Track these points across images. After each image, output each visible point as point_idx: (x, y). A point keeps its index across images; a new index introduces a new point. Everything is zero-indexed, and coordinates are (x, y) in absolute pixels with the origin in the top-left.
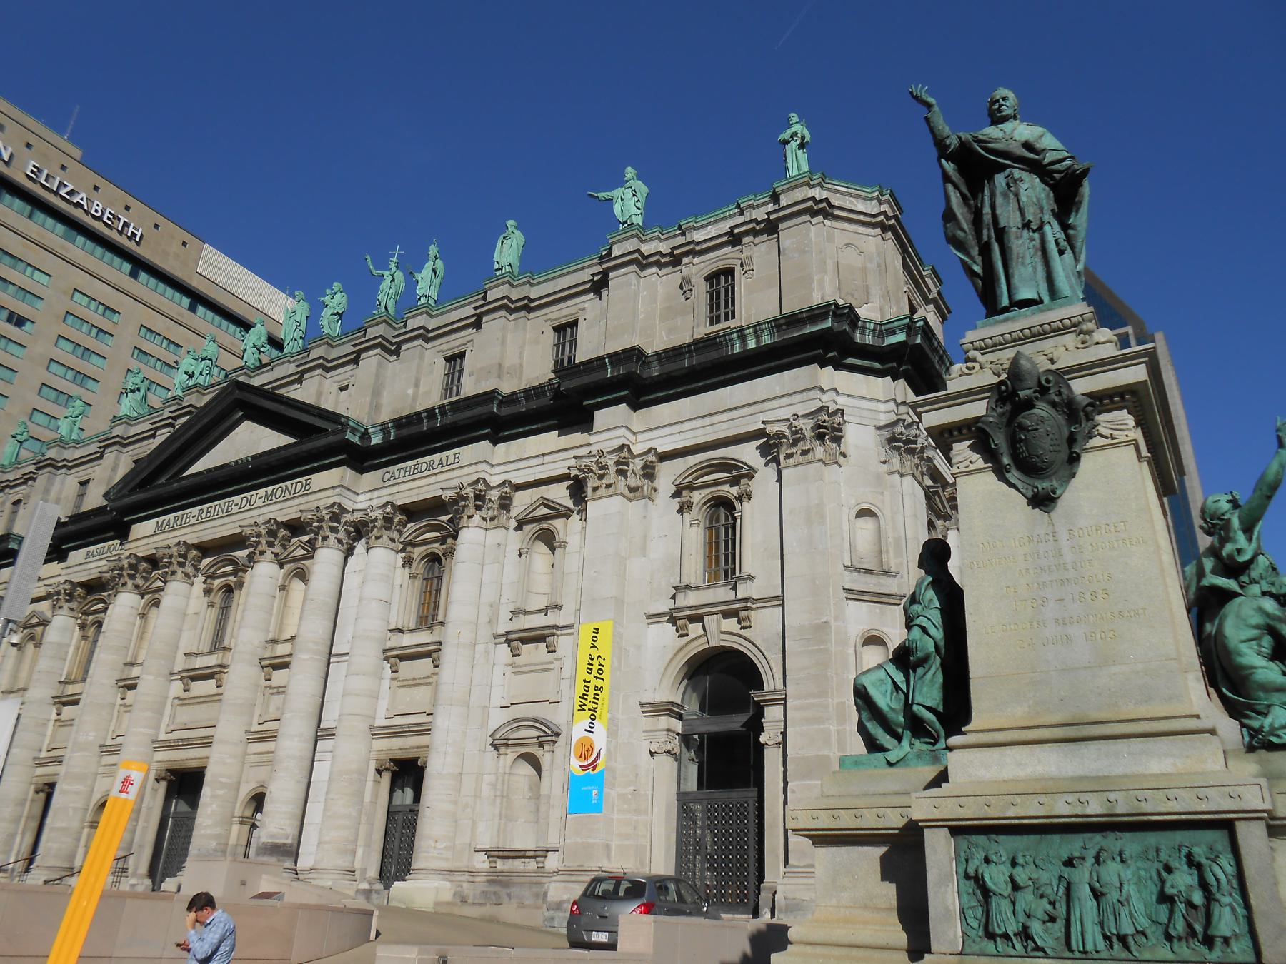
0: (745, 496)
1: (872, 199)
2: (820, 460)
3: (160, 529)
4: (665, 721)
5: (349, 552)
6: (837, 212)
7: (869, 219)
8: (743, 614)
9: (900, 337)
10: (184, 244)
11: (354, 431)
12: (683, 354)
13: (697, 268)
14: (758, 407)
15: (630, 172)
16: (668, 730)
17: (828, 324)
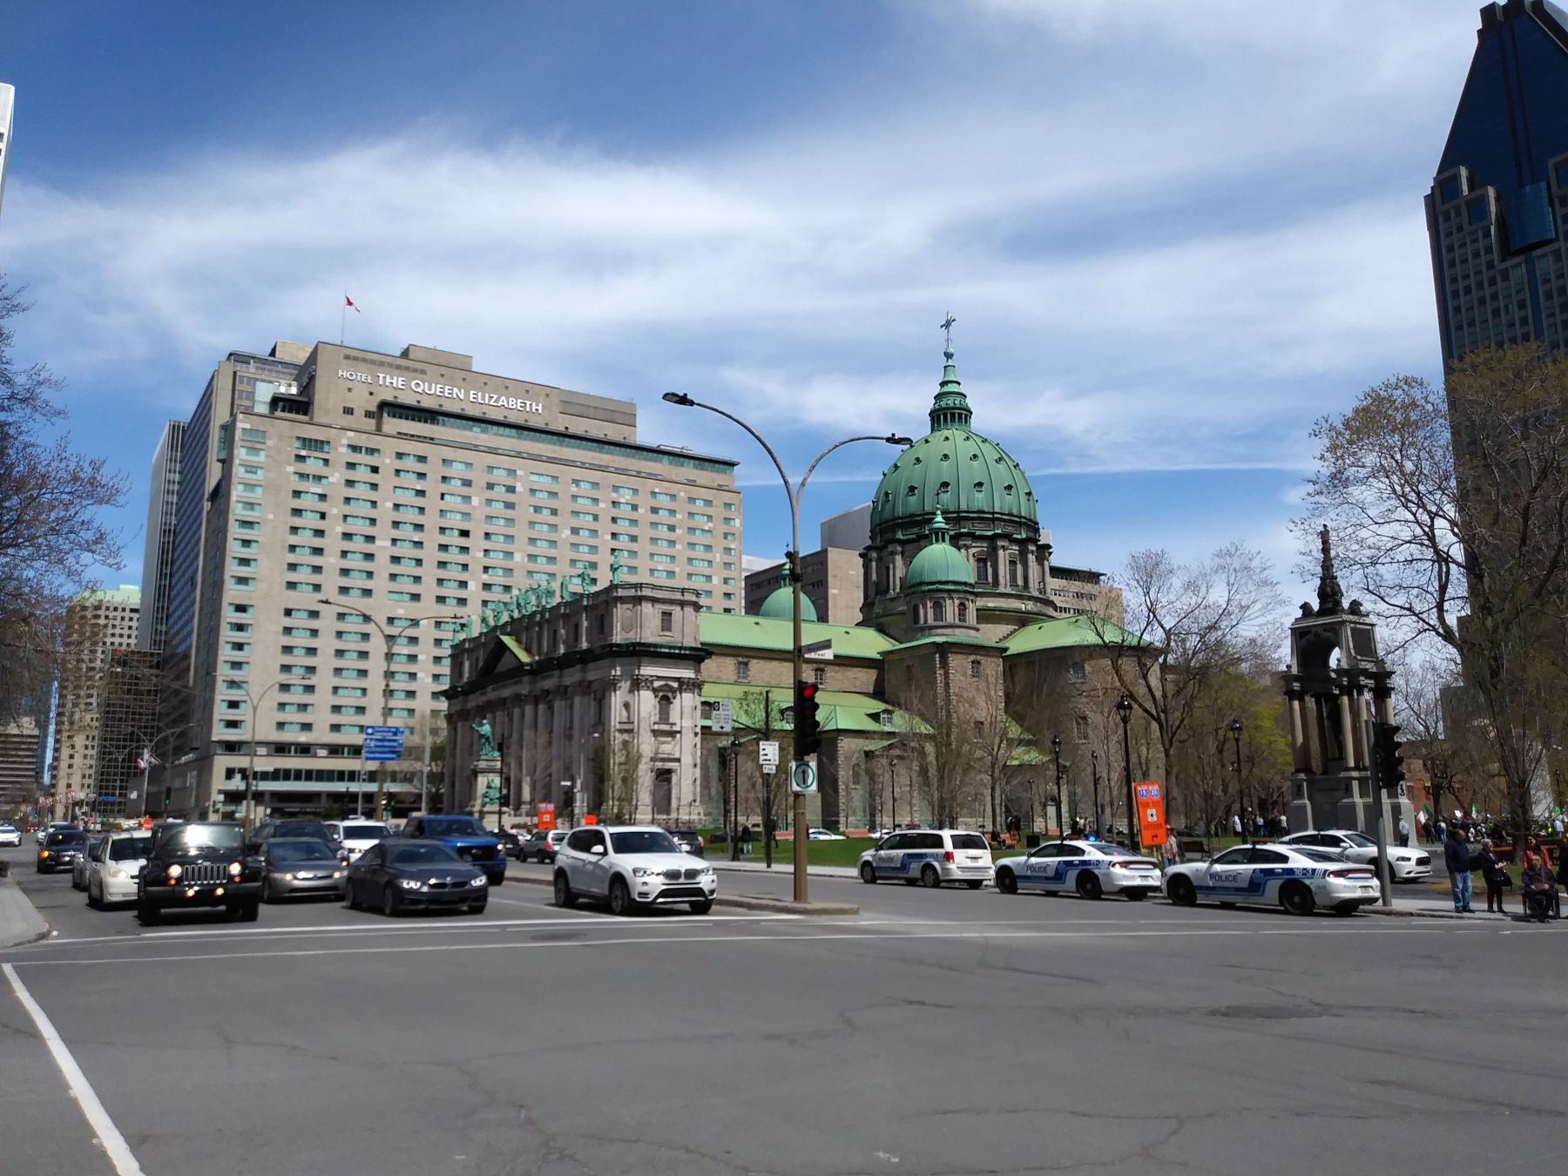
5: (536, 705)
10: (547, 395)
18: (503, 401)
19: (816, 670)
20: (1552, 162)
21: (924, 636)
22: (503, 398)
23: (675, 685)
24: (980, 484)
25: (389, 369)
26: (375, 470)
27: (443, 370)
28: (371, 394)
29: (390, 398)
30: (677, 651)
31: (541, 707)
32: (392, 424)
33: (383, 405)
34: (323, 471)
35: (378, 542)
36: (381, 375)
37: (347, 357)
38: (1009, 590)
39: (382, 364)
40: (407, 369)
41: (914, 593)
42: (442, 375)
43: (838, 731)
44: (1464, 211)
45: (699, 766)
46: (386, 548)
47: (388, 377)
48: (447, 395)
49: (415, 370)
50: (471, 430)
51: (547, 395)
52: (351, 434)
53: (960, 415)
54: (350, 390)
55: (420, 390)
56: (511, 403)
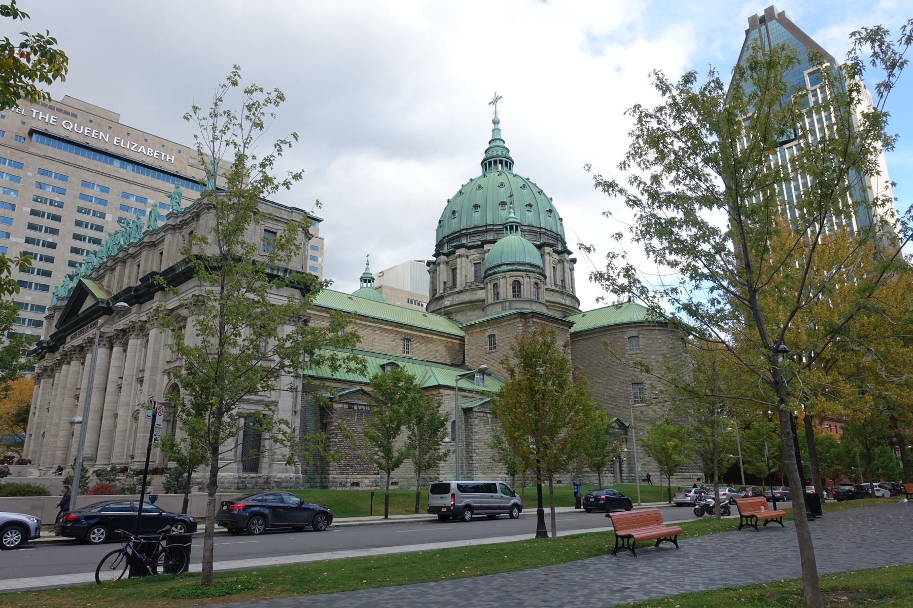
5: (111, 348)
10: (180, 152)
11: (102, 302)
13: (186, 231)
18: (142, 149)
19: (404, 340)
21: (503, 309)
22: (142, 147)
24: (530, 205)
25: (43, 108)
28: (23, 123)
29: (40, 127)
31: (116, 349)
32: (38, 146)
33: (32, 132)
35: (12, 239)
36: (35, 111)
38: (553, 287)
40: (60, 110)
41: (495, 273)
42: (91, 121)
43: (439, 387)
45: (299, 413)
46: (21, 244)
47: (41, 113)
49: (67, 113)
50: (112, 164)
51: (180, 152)
55: (68, 128)
56: (148, 152)
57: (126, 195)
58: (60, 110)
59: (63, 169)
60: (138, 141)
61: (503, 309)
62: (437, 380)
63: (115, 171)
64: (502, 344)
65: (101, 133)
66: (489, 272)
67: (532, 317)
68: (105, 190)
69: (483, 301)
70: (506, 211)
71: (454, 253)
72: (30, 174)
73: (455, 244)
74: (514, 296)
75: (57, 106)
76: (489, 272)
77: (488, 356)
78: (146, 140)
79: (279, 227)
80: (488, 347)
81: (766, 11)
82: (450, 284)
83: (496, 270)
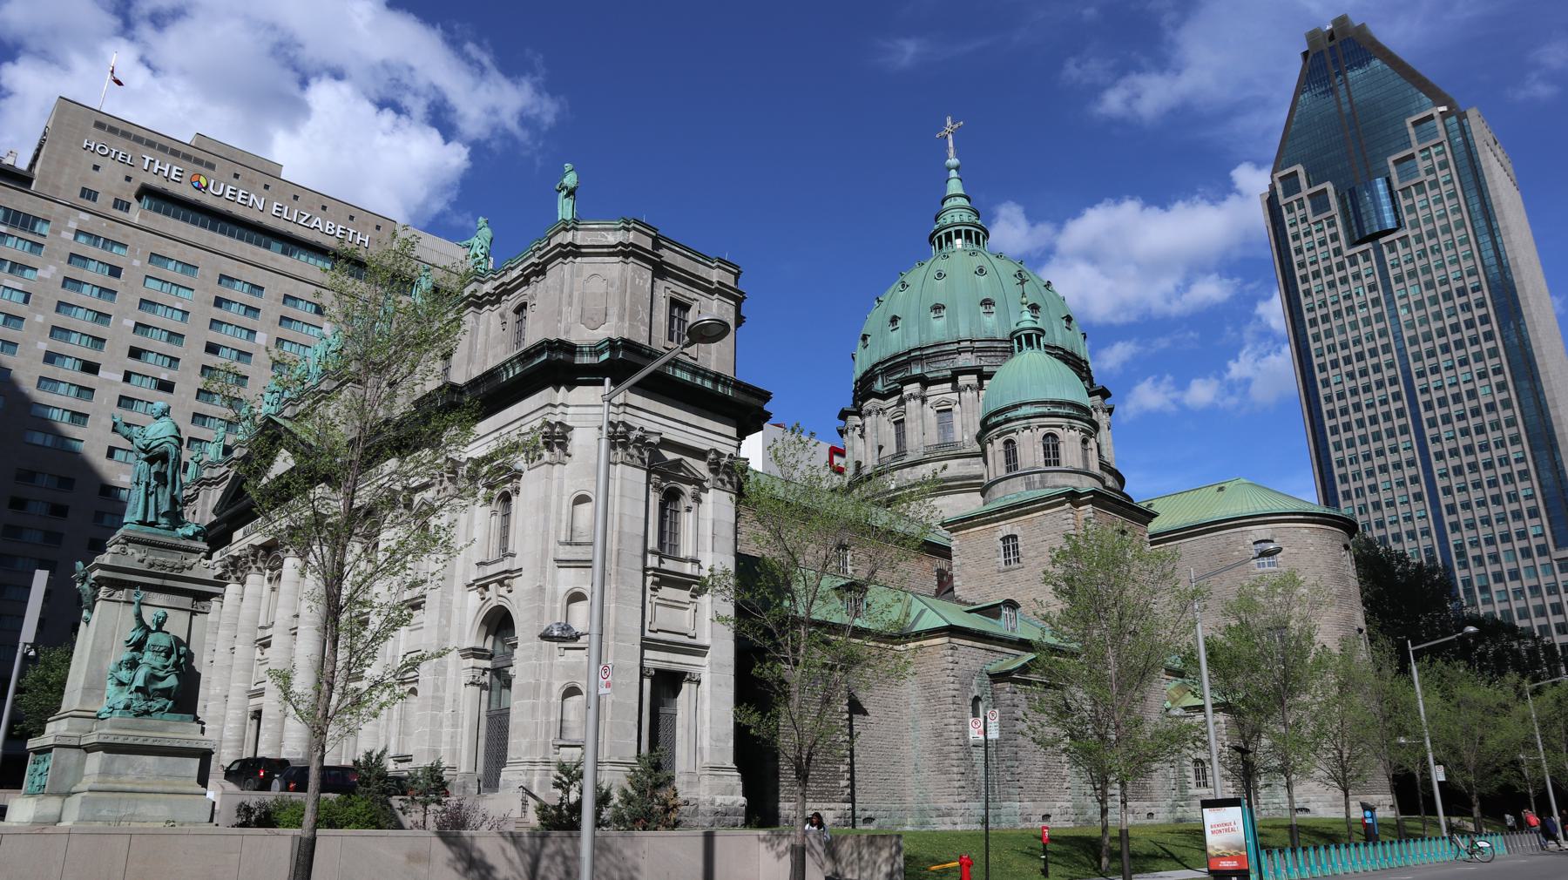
0: (517, 491)
1: (620, 229)
2: (546, 463)
3: (246, 535)
4: (472, 662)
6: (583, 250)
7: (611, 250)
8: (506, 582)
9: (606, 356)
10: (378, 228)
12: (479, 384)
13: (510, 303)
14: (522, 422)
15: (481, 220)
16: (473, 668)
17: (545, 357)
20: (1390, 160)
22: (318, 219)
23: (701, 468)
26: (115, 272)
27: (239, 170)
28: (128, 179)
29: (156, 182)
30: (708, 384)
34: (31, 259)
37: (99, 125)
39: (151, 144)
40: (187, 157)
41: (1008, 421)
42: (236, 176)
44: (1307, 203)
47: (157, 162)
48: (239, 200)
49: (198, 162)
50: (268, 247)
52: (85, 217)
53: (977, 234)
54: (96, 168)
56: (328, 227)
57: (287, 298)
58: (187, 157)
59: (190, 255)
60: (312, 208)
61: (1029, 486)
62: (946, 621)
63: (272, 259)
64: (1032, 554)
65: (253, 196)
66: (994, 420)
67: (1091, 502)
68: (257, 289)
69: (981, 477)
70: (993, 316)
71: (900, 392)
72: (137, 263)
73: (898, 376)
74: (1047, 463)
75: (185, 150)
76: (994, 420)
77: (1002, 576)
78: (324, 208)
79: (696, 296)
80: (1002, 559)
81: (1335, 22)
82: (891, 448)
83: (1009, 415)
